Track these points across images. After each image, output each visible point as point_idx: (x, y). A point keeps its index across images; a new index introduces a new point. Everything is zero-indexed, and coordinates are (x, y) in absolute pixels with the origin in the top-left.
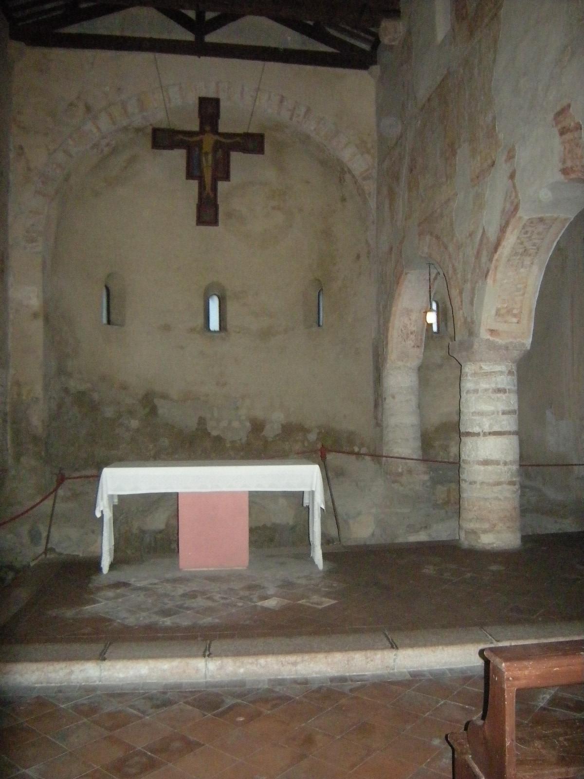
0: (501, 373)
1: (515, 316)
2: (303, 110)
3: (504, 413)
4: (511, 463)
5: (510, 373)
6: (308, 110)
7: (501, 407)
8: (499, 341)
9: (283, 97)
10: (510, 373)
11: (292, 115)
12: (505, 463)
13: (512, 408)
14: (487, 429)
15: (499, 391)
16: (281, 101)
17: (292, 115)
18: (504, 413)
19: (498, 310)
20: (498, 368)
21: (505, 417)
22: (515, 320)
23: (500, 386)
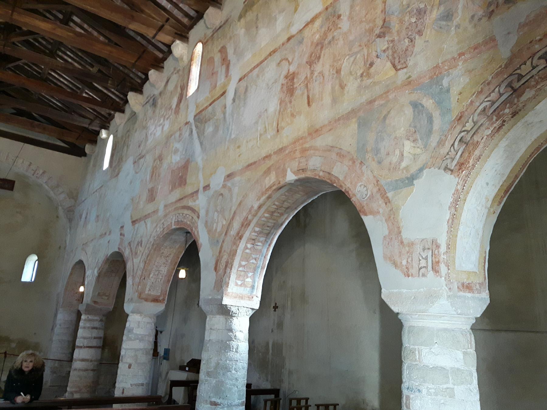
0: (97, 320)
1: (107, 296)
2: (41, 172)
3: (95, 338)
4: (95, 361)
5: (101, 320)
6: (44, 172)
7: (94, 335)
8: (97, 306)
9: (31, 163)
10: (101, 320)
11: (35, 173)
12: (91, 361)
13: (99, 336)
14: (85, 345)
15: (96, 328)
16: (29, 165)
17: (35, 173)
18: (95, 338)
19: (99, 293)
20: (96, 318)
21: (95, 340)
22: (106, 298)
23: (95, 326)
